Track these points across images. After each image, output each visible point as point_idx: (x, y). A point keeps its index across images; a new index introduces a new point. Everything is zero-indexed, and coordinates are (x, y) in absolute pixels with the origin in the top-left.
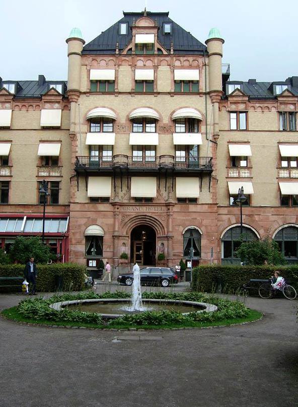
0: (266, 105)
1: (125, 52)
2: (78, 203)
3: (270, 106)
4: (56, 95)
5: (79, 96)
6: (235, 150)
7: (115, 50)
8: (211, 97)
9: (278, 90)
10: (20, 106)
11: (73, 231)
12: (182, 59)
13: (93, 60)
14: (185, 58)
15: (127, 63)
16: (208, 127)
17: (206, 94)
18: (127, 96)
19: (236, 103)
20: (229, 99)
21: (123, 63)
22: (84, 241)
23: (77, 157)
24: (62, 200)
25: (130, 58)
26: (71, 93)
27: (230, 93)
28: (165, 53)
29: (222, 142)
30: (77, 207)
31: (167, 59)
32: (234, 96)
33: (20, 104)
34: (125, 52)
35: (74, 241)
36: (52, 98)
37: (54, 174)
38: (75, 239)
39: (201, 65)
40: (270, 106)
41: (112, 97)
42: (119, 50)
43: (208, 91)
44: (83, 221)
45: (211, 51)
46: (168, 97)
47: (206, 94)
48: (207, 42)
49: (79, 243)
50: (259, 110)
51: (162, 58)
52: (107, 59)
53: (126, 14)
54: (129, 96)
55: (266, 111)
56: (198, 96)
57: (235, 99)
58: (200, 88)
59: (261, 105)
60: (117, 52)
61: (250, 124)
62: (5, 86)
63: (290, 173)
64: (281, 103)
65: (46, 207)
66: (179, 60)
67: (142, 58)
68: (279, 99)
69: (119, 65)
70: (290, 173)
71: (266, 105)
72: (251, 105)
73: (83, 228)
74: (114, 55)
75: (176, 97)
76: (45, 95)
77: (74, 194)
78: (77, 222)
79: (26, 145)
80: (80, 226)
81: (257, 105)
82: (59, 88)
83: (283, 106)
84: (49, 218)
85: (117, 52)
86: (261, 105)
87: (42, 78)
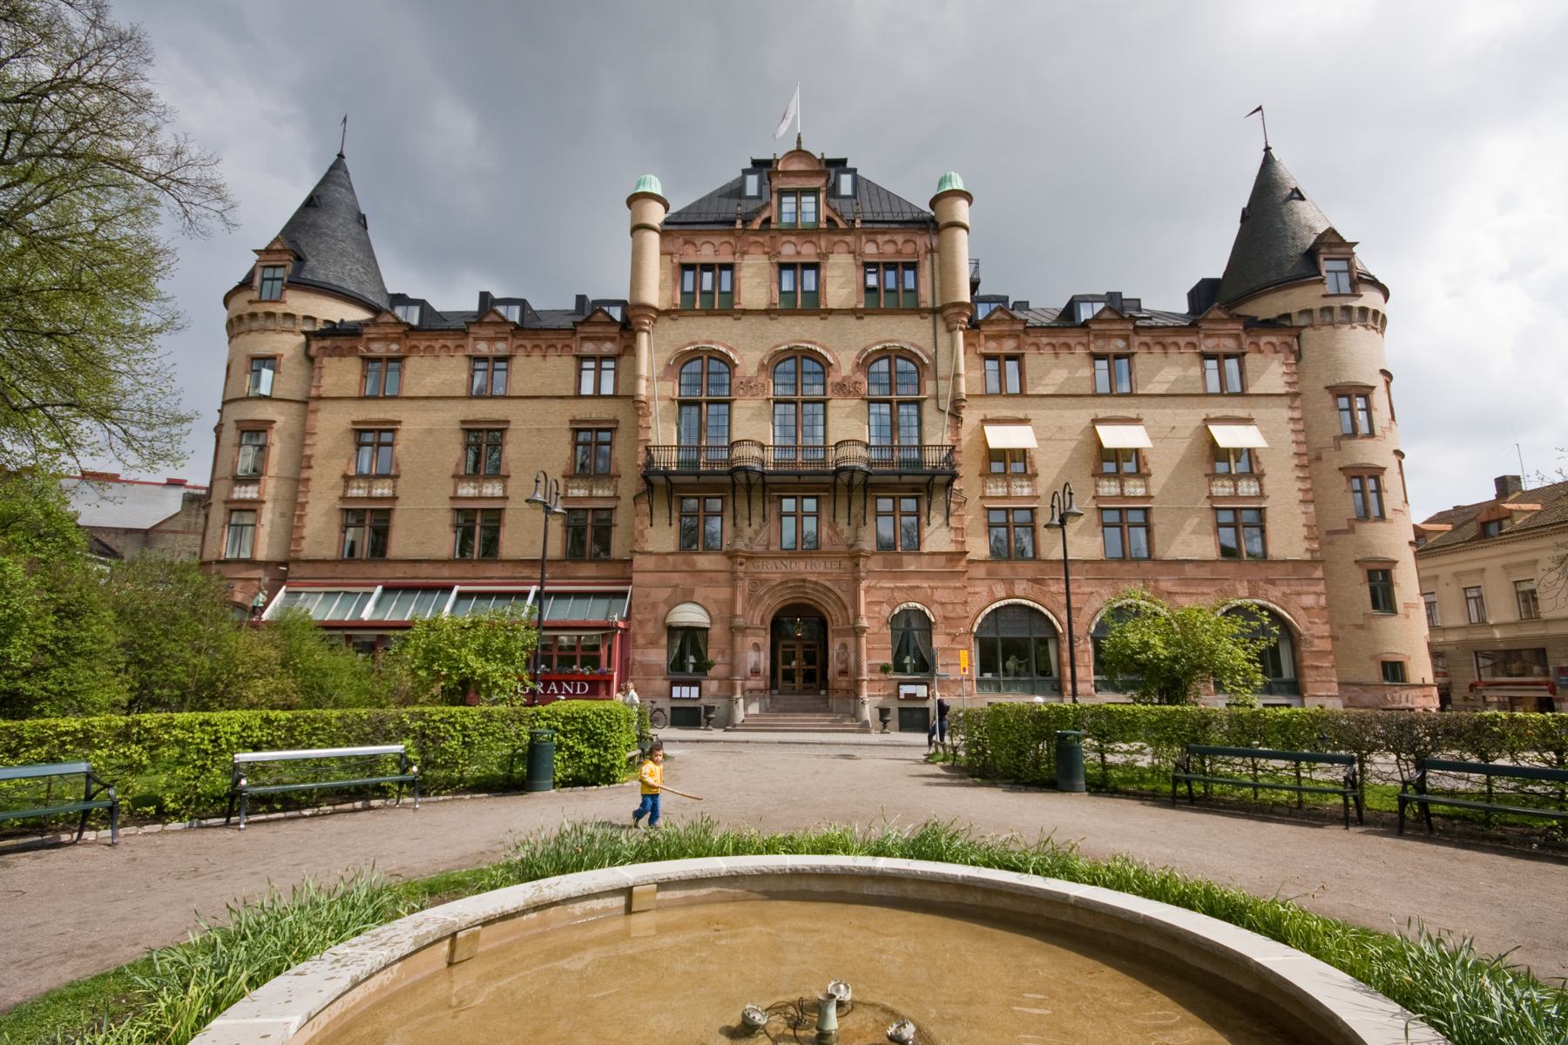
0: (1062, 340)
1: (756, 225)
2: (650, 553)
3: (1072, 342)
4: (608, 324)
5: (655, 321)
6: (999, 438)
7: (734, 223)
8: (945, 319)
9: (1086, 313)
10: (529, 346)
11: (638, 617)
12: (880, 239)
13: (686, 242)
14: (887, 238)
15: (760, 250)
16: (941, 383)
17: (935, 311)
18: (760, 318)
19: (998, 337)
20: (983, 328)
21: (752, 249)
22: (664, 641)
23: (648, 449)
24: (618, 548)
25: (767, 238)
26: (637, 312)
27: (980, 317)
28: (842, 225)
29: (970, 417)
30: (650, 563)
31: (849, 239)
32: (992, 323)
33: (528, 344)
34: (756, 225)
35: (640, 640)
36: (599, 329)
37: (600, 493)
38: (644, 636)
39: (922, 252)
40: (1072, 342)
41: (728, 321)
42: (744, 222)
43: (938, 305)
44: (662, 594)
45: (943, 221)
46: (851, 321)
47: (935, 311)
48: (933, 204)
49: (653, 643)
50: (1049, 350)
51: (836, 238)
52: (717, 240)
53: (755, 163)
54: (765, 320)
55: (1063, 352)
56: (917, 318)
57: (995, 329)
58: (922, 299)
59: (1054, 341)
60: (739, 225)
61: (1028, 381)
62: (501, 309)
63: (1122, 487)
64: (1097, 336)
65: (295, 406)
66: (875, 242)
67: (793, 239)
68: (1094, 327)
69: (744, 253)
70: (1122, 487)
71: (1062, 340)
72: (1030, 340)
73: (662, 609)
74: (731, 233)
75: (867, 319)
76: (582, 323)
77: (642, 534)
78: (647, 596)
79: (539, 430)
80: (654, 605)
81: (1045, 340)
82: (617, 313)
83: (1100, 343)
84: (531, 563)
85: (739, 225)
86: (1054, 341)
87: (581, 299)
